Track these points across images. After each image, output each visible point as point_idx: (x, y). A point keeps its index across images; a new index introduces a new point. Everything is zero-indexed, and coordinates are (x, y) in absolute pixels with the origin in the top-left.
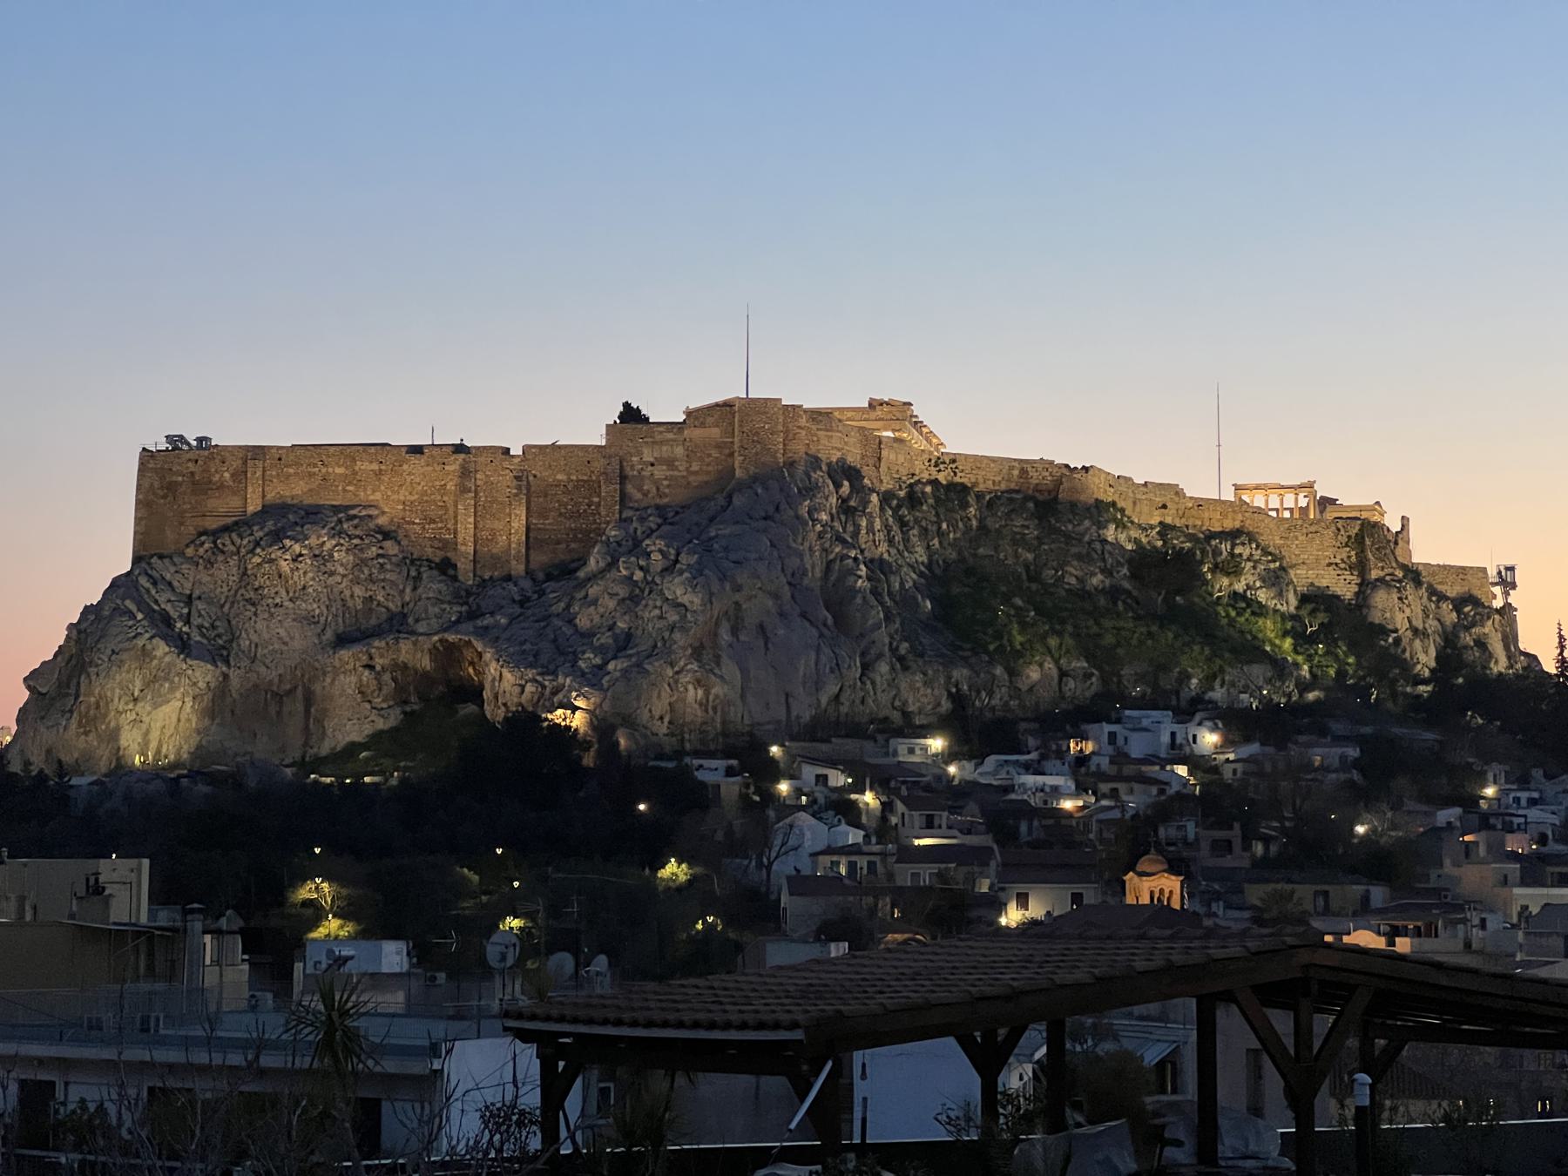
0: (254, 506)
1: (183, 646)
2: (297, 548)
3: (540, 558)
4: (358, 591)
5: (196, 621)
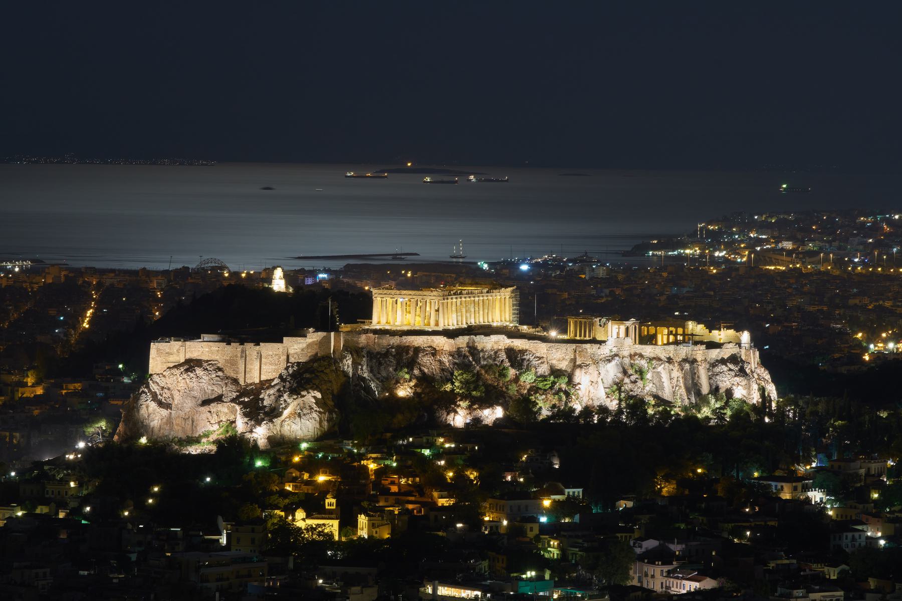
0: (182, 360)
1: (161, 404)
2: (192, 375)
3: (263, 378)
4: (210, 387)
5: (164, 395)
